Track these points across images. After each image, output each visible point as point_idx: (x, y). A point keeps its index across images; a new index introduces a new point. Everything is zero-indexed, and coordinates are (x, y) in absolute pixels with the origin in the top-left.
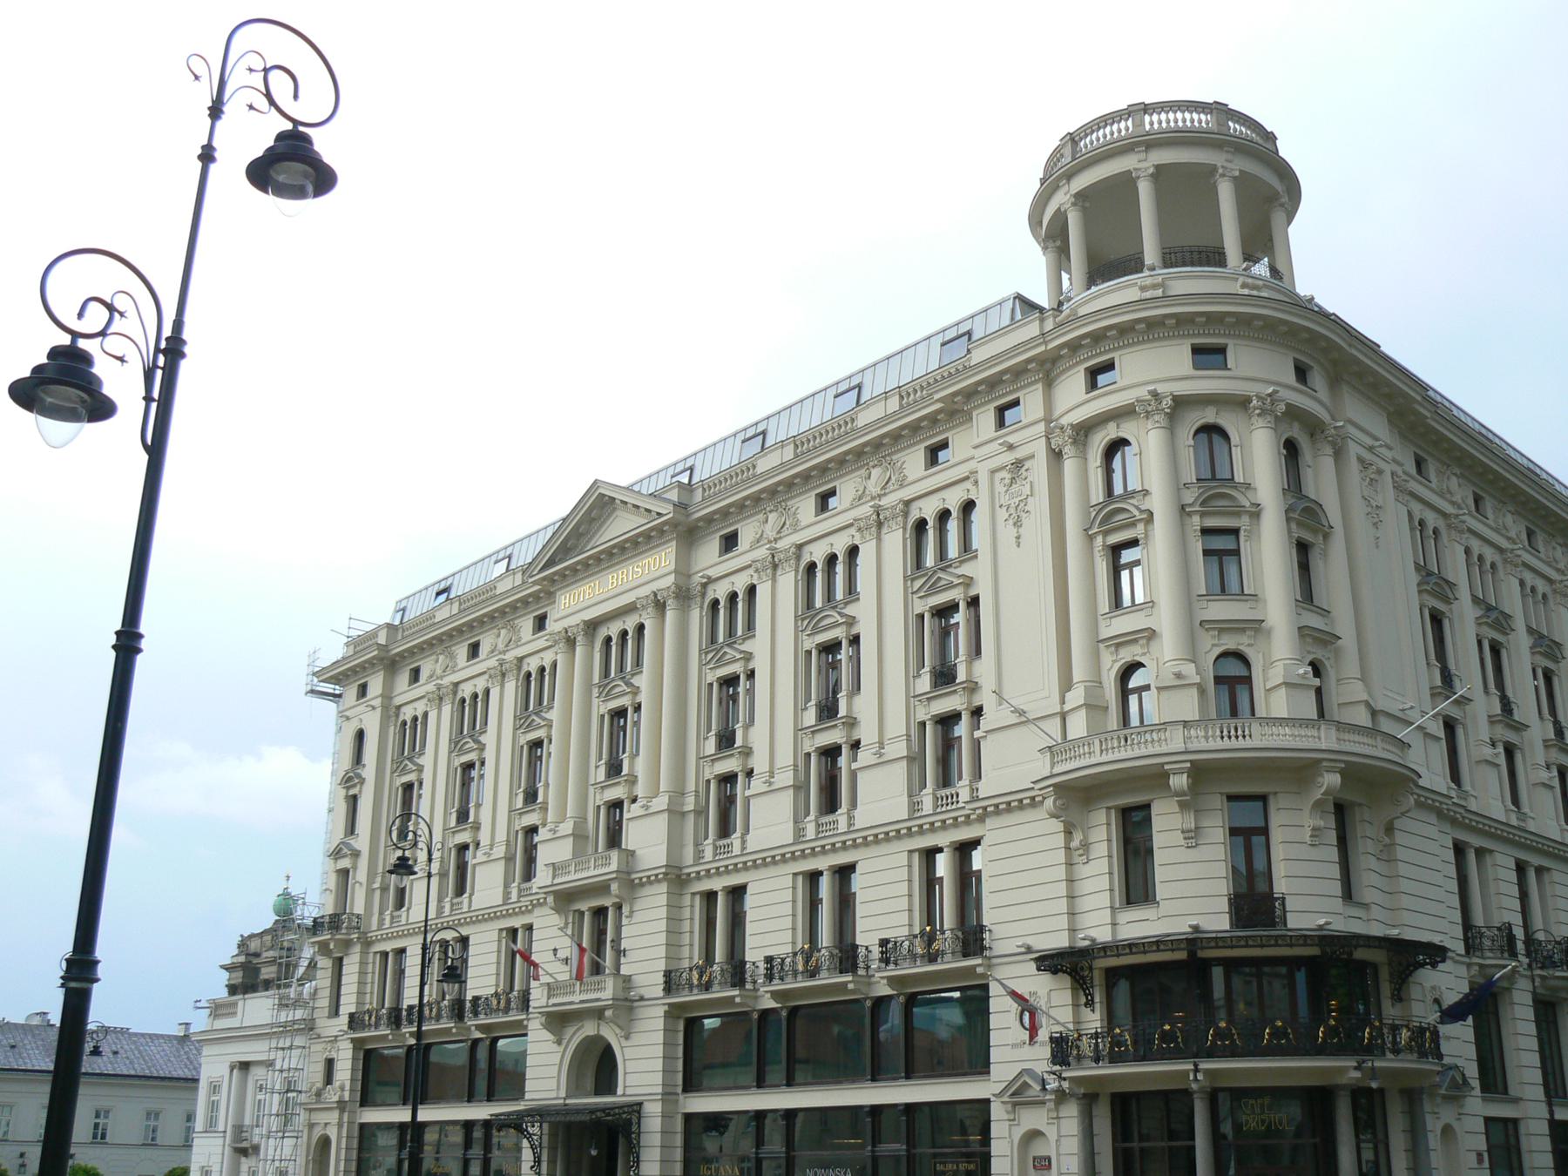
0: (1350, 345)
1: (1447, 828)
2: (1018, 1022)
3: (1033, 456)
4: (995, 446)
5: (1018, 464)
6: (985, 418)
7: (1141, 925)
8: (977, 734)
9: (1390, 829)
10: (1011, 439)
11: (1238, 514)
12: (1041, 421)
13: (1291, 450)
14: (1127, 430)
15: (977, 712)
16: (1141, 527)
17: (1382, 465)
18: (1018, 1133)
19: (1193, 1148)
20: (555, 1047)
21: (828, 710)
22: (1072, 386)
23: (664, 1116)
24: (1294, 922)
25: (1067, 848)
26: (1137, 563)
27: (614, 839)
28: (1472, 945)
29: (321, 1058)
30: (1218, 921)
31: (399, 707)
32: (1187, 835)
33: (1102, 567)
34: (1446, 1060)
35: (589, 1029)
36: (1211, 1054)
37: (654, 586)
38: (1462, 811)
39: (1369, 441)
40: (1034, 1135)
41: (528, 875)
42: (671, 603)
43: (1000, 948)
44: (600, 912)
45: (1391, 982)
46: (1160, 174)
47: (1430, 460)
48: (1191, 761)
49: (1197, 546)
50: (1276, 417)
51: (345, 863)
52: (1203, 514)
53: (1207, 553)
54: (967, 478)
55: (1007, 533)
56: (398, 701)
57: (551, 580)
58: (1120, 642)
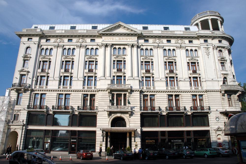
3: (210, 48)
5: (208, 48)
6: (202, 41)
14: (223, 49)
31: (41, 45)
35: (119, 115)
37: (133, 43)
56: (41, 44)
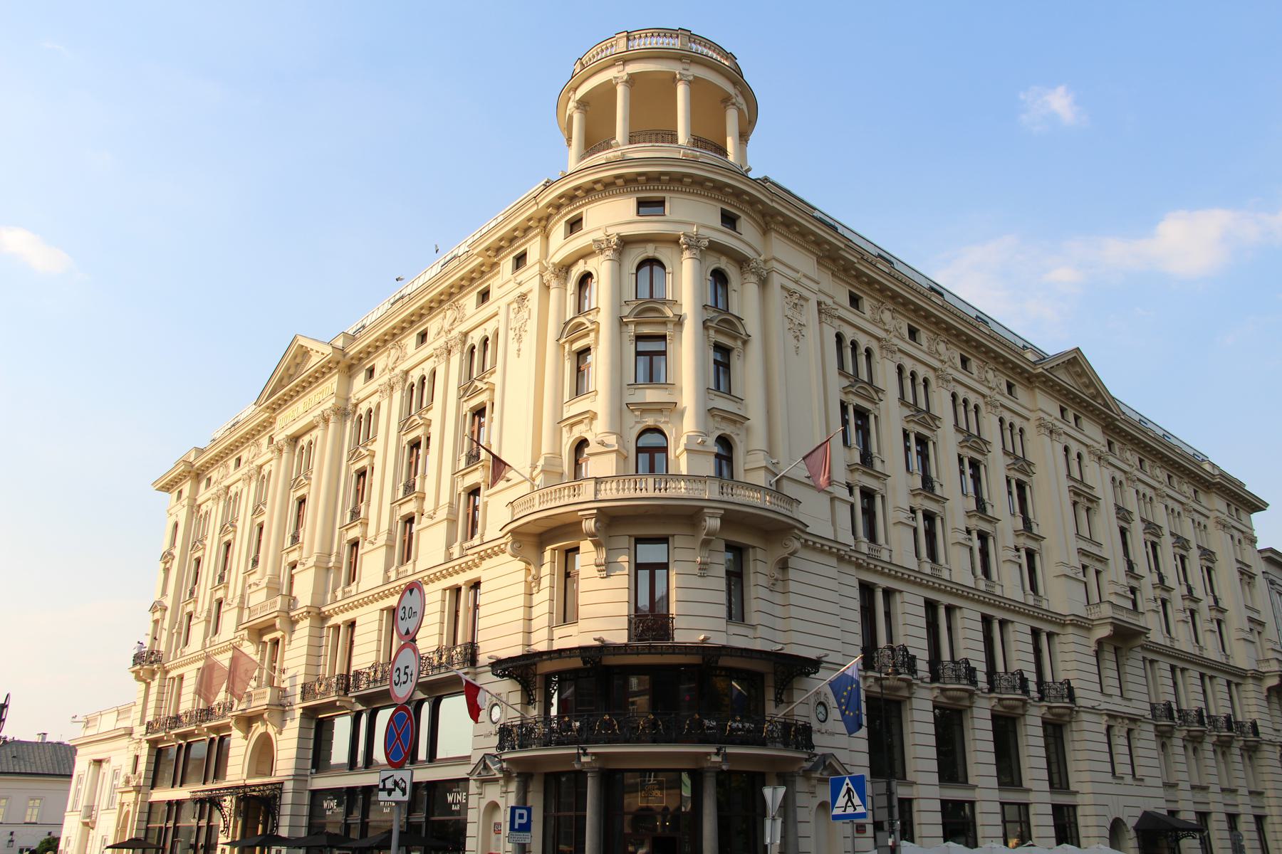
0: (772, 200)
1: (852, 570)
2: (488, 717)
3: (531, 291)
5: (523, 297)
9: (784, 565)
10: (519, 280)
11: (665, 323)
12: (536, 264)
13: (719, 277)
16: (592, 335)
17: (806, 293)
18: (484, 803)
19: (585, 816)
23: (295, 791)
24: (680, 637)
25: (526, 581)
29: (132, 756)
30: (619, 635)
32: (599, 568)
33: (568, 366)
34: (818, 751)
36: (596, 742)
38: (865, 558)
42: (332, 418)
43: (483, 659)
44: (276, 642)
45: (775, 687)
46: (632, 80)
47: (865, 297)
48: (598, 509)
49: (630, 350)
50: (701, 250)
51: (158, 615)
52: (637, 324)
53: (638, 354)
55: (513, 346)
58: (574, 422)
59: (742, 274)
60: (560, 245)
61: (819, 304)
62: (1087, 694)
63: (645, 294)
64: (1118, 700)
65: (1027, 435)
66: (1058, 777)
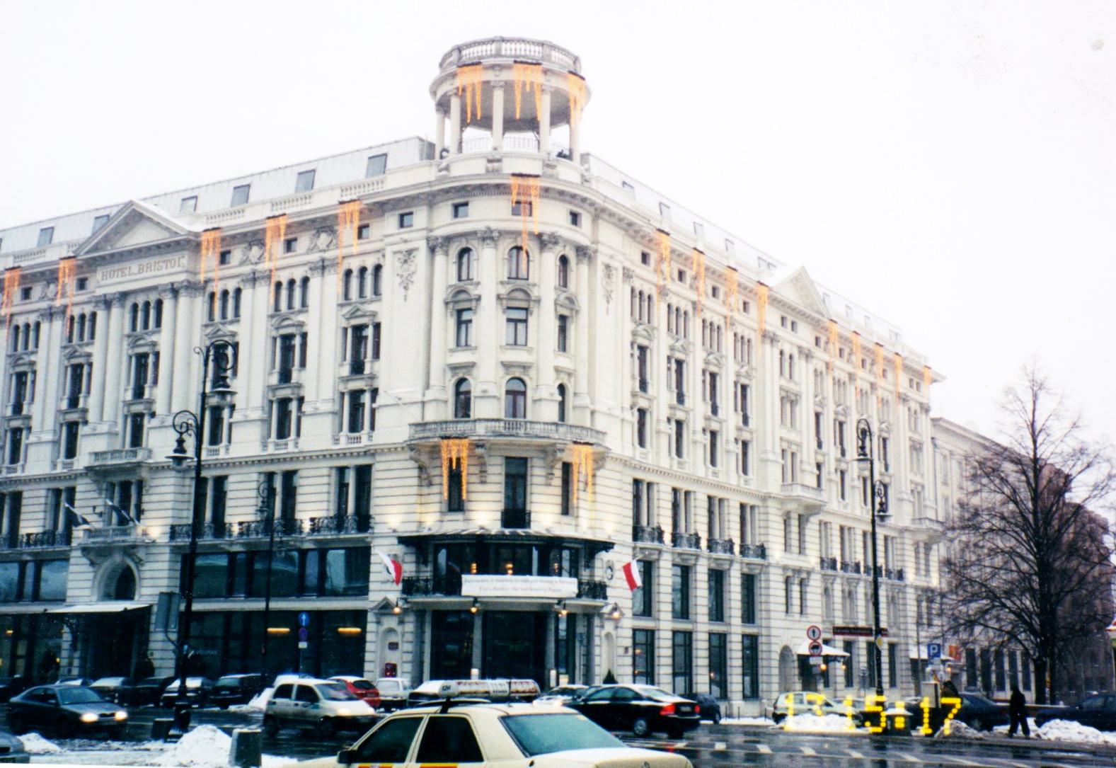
3: (417, 249)
4: (396, 239)
5: (410, 252)
6: (391, 222)
7: (454, 525)
8: (374, 405)
10: (406, 236)
14: (473, 244)
15: (375, 392)
16: (473, 304)
20: (91, 569)
21: (285, 376)
22: (445, 211)
25: (419, 477)
26: (470, 321)
27: (137, 439)
28: (637, 533)
33: (452, 322)
35: (117, 558)
39: (611, 252)
40: (391, 631)
41: (71, 452)
44: (125, 487)
54: (379, 251)
57: (94, 259)
58: (454, 368)
59: (578, 255)
60: (444, 221)
61: (624, 268)
62: (776, 553)
63: (514, 275)
64: (796, 556)
65: (753, 342)
66: (749, 615)
